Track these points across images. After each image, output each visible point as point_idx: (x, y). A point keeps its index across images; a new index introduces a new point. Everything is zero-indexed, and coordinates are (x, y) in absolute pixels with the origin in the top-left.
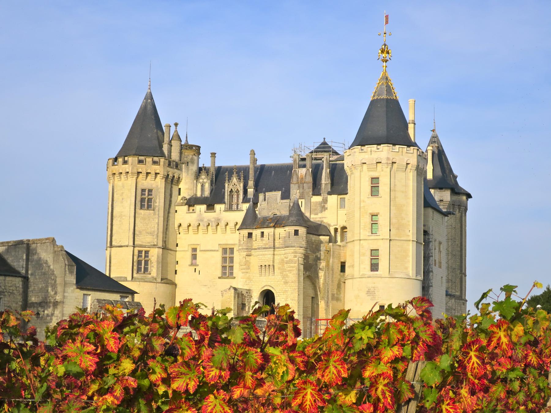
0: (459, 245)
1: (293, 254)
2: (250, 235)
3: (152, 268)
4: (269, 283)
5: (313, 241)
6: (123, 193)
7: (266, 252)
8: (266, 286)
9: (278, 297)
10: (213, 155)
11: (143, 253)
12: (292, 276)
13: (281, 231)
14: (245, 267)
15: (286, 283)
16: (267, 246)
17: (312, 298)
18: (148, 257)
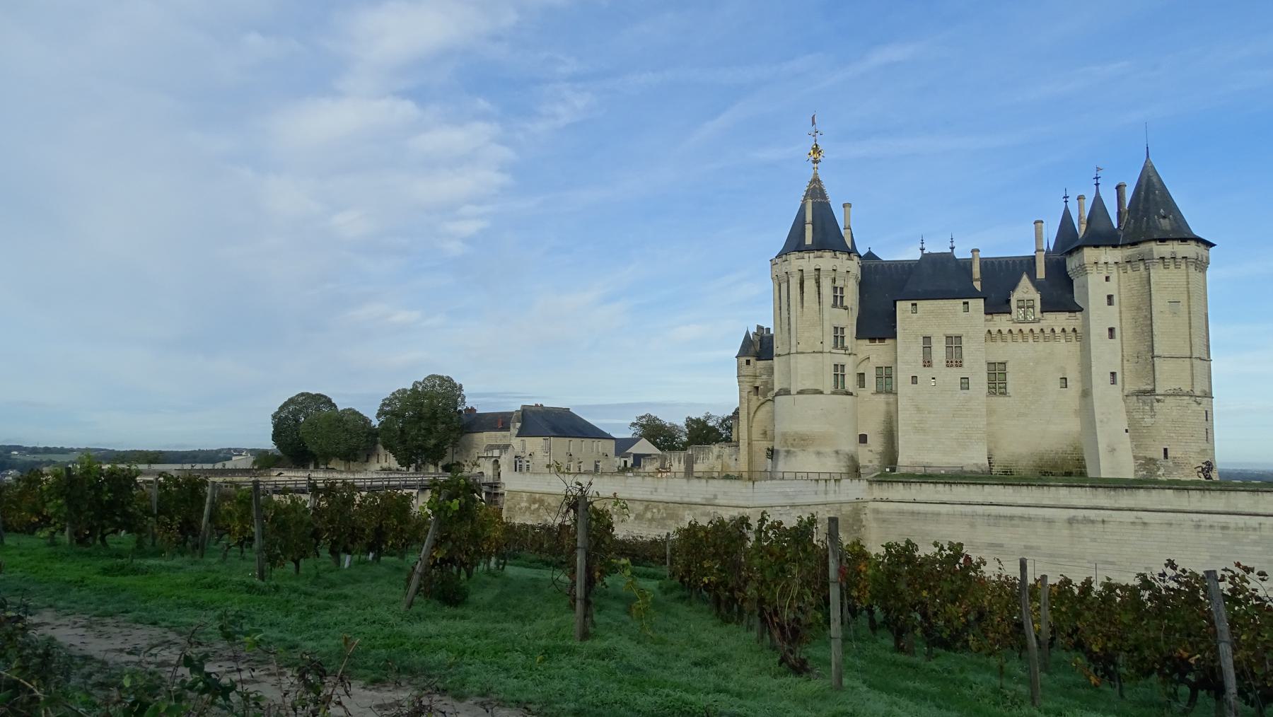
0: (1149, 316)
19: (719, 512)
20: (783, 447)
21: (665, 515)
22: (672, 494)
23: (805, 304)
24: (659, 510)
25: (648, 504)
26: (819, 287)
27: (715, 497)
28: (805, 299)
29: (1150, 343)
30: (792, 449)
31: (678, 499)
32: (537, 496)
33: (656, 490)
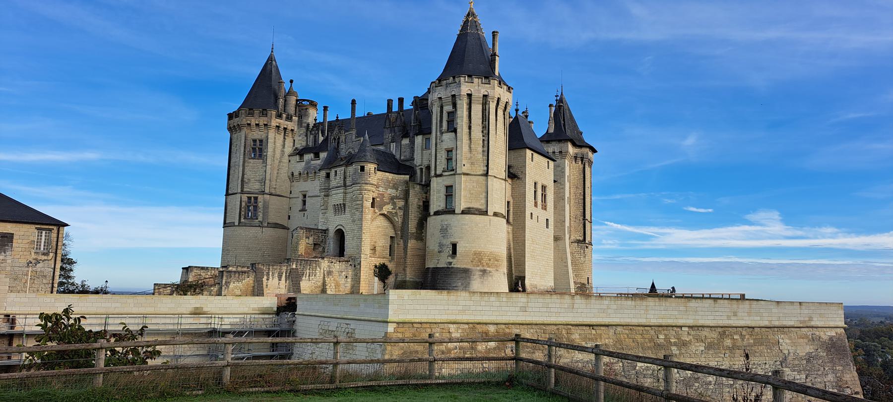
0: (582, 194)
1: (359, 191)
2: (328, 175)
3: (259, 213)
4: (341, 222)
5: (390, 180)
6: (237, 145)
7: (338, 191)
8: (338, 226)
9: (347, 237)
10: (325, 108)
11: (252, 199)
12: (359, 214)
13: (351, 169)
14: (323, 207)
15: (354, 221)
16: (339, 185)
17: (391, 237)
18: (256, 203)
19: (817, 333)
20: (478, 266)
21: (752, 341)
22: (759, 318)
23: (498, 132)
24: (742, 337)
25: (724, 331)
26: (504, 118)
27: (811, 319)
28: (498, 126)
29: (582, 211)
30: (488, 269)
31: (766, 323)
32: (492, 329)
33: (735, 314)
